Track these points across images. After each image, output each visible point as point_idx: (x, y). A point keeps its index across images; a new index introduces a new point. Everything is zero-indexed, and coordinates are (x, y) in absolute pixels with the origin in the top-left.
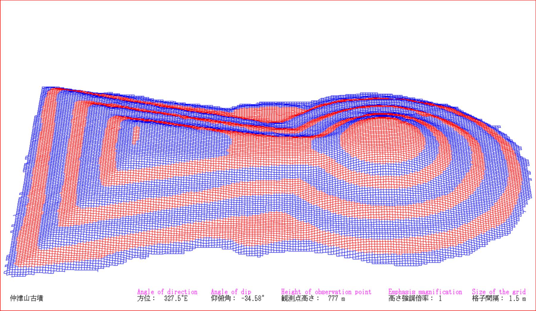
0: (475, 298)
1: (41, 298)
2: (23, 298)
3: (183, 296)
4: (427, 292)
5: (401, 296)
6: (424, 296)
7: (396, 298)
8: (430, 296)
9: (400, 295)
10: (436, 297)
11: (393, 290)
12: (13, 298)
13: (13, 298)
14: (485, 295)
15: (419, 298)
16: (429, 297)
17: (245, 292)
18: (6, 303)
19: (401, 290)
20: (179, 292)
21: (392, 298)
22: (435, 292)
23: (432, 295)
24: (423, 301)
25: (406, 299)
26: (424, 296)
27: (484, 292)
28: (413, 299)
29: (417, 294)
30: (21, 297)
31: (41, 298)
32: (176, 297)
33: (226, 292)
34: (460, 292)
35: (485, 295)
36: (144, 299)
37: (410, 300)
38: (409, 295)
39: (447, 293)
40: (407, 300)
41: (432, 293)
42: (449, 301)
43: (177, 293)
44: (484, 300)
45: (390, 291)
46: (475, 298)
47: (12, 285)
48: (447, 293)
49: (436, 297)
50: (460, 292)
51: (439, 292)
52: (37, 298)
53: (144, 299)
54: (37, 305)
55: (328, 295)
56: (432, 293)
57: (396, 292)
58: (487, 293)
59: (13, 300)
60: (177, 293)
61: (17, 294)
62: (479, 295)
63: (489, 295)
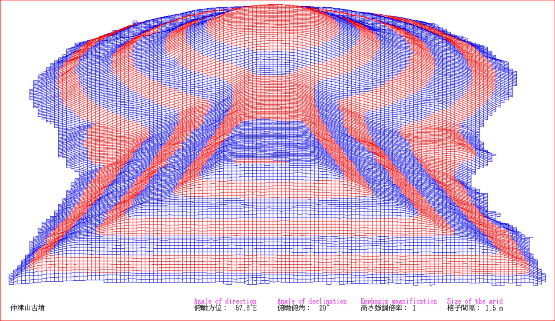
0: (450, 308)
1: (42, 308)
2: (24, 308)
3: (252, 305)
4: (400, 301)
5: (374, 305)
6: (397, 306)
7: (368, 307)
8: (403, 306)
9: (373, 305)
10: (410, 307)
11: (365, 299)
12: (13, 307)
13: (13, 307)
14: (461, 305)
15: (393, 308)
16: (403, 307)
17: (229, 302)
18: (6, 313)
19: (374, 299)
20: (237, 301)
21: (364, 308)
22: (409, 302)
23: (406, 305)
24: (396, 311)
25: (379, 308)
26: (397, 306)
27: (460, 301)
28: (386, 308)
29: (390, 303)
30: (22, 306)
31: (42, 308)
32: (244, 307)
33: (293, 301)
34: (434, 302)
35: (461, 305)
36: (215, 309)
37: (383, 310)
38: (381, 304)
39: (421, 302)
40: (380, 309)
41: (406, 302)
42: (423, 311)
43: (235, 302)
44: (460, 309)
45: (362, 301)
46: (450, 308)
47: (13, 294)
48: (421, 302)
49: (410, 307)
50: (434, 302)
51: (413, 302)
52: (38, 308)
53: (215, 309)
54: (39, 314)
55: (319, 304)
56: (406, 302)
57: (368, 302)
58: (463, 303)
59: (13, 310)
60: (235, 302)
61: (18, 303)
62: (454, 304)
63: (465, 304)
